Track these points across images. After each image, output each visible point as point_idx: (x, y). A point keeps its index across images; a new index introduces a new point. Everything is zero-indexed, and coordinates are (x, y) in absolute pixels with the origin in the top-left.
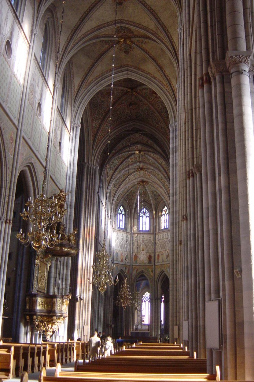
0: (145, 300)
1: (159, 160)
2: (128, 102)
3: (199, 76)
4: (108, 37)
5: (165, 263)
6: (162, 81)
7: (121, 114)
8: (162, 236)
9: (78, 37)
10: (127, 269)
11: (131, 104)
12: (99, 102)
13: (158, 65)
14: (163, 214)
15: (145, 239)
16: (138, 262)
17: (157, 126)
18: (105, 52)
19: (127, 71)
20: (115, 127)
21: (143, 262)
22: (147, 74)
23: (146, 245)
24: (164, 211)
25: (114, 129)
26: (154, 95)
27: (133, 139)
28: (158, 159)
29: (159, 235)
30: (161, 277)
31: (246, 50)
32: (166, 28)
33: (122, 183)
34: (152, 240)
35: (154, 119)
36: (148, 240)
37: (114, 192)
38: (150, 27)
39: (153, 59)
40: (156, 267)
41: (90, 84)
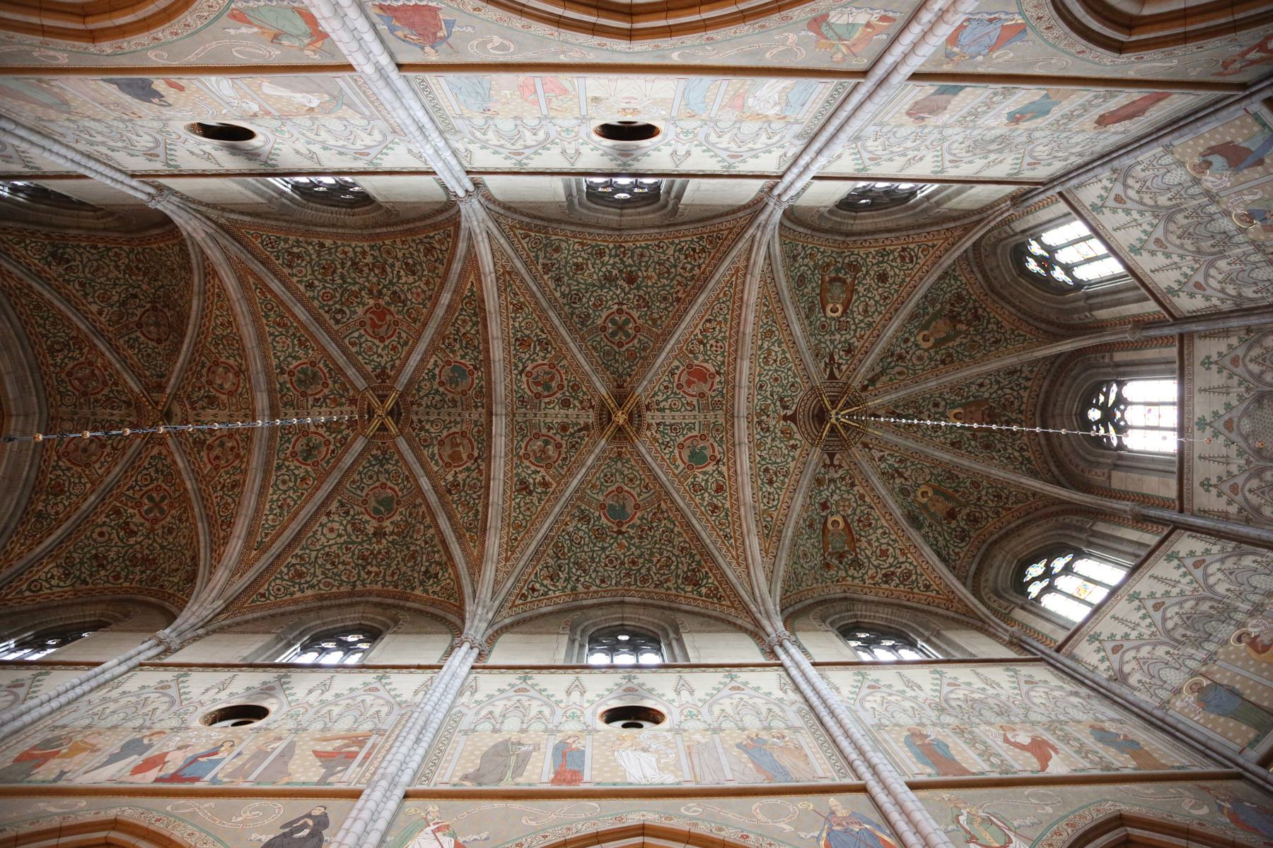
1: (418, 312)
15: (1218, 403)
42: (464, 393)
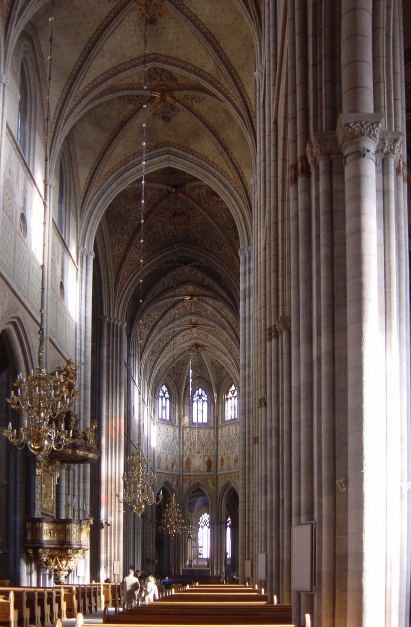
0: (203, 525)
1: (223, 311)
2: (170, 211)
3: (290, 162)
4: (132, 89)
5: (233, 471)
6: (227, 171)
7: (159, 232)
8: (227, 431)
9: (81, 89)
10: (175, 481)
11: (175, 215)
12: (121, 211)
13: (221, 142)
14: (229, 397)
15: (202, 436)
16: (192, 469)
17: (218, 253)
18: (129, 119)
19: (168, 153)
20: (151, 255)
21: (199, 470)
22: (202, 159)
23: (203, 445)
24: (230, 393)
25: (150, 258)
26: (214, 197)
27: (180, 275)
28: (220, 308)
29: (224, 430)
30: (225, 492)
31: (373, 112)
32: (234, 70)
33: (163, 349)
34: (212, 437)
35: (214, 241)
36: (206, 436)
37: (153, 362)
38: (207, 69)
39: (211, 131)
40: (219, 477)
41: (106, 179)
42: (199, 308)
